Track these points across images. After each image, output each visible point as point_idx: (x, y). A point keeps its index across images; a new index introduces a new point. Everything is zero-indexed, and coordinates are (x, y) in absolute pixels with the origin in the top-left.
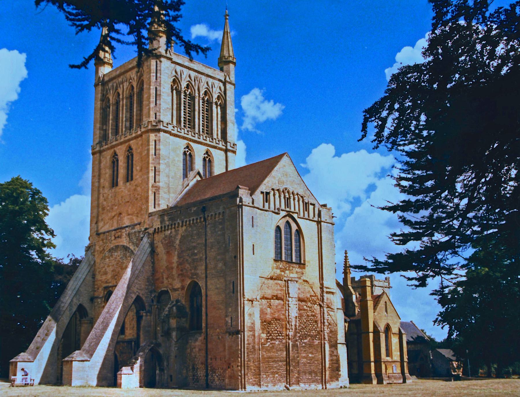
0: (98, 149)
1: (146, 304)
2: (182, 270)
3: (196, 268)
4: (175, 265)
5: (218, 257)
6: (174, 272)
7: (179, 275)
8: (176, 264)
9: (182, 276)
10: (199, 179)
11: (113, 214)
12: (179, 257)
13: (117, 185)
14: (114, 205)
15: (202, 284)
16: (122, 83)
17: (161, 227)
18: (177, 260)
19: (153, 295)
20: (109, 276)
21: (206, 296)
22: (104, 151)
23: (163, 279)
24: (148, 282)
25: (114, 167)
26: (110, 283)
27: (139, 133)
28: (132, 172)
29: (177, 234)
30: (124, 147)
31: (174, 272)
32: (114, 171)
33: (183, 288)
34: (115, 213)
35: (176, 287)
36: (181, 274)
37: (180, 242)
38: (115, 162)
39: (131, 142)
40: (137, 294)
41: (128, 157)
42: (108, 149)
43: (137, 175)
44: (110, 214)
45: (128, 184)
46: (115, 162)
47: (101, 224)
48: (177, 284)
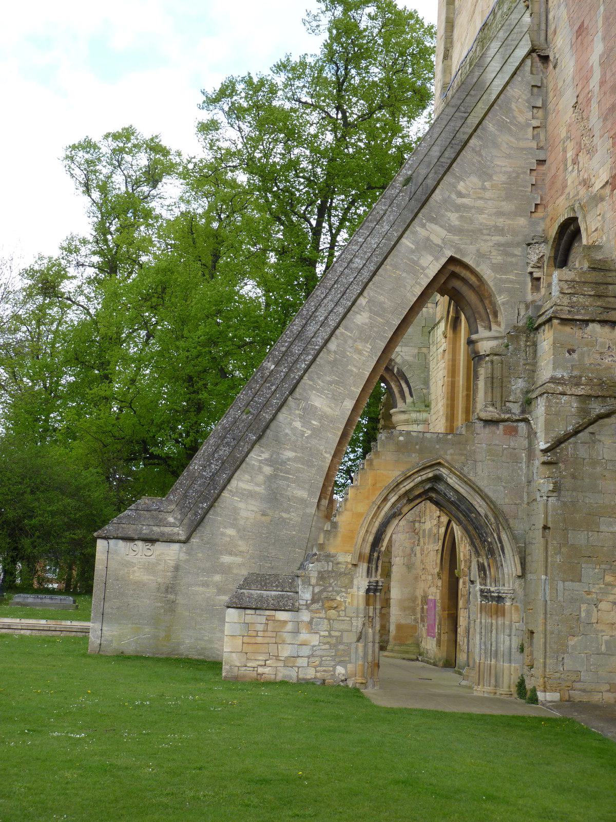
1: (500, 299)
19: (534, 258)
24: (508, 197)
40: (449, 253)
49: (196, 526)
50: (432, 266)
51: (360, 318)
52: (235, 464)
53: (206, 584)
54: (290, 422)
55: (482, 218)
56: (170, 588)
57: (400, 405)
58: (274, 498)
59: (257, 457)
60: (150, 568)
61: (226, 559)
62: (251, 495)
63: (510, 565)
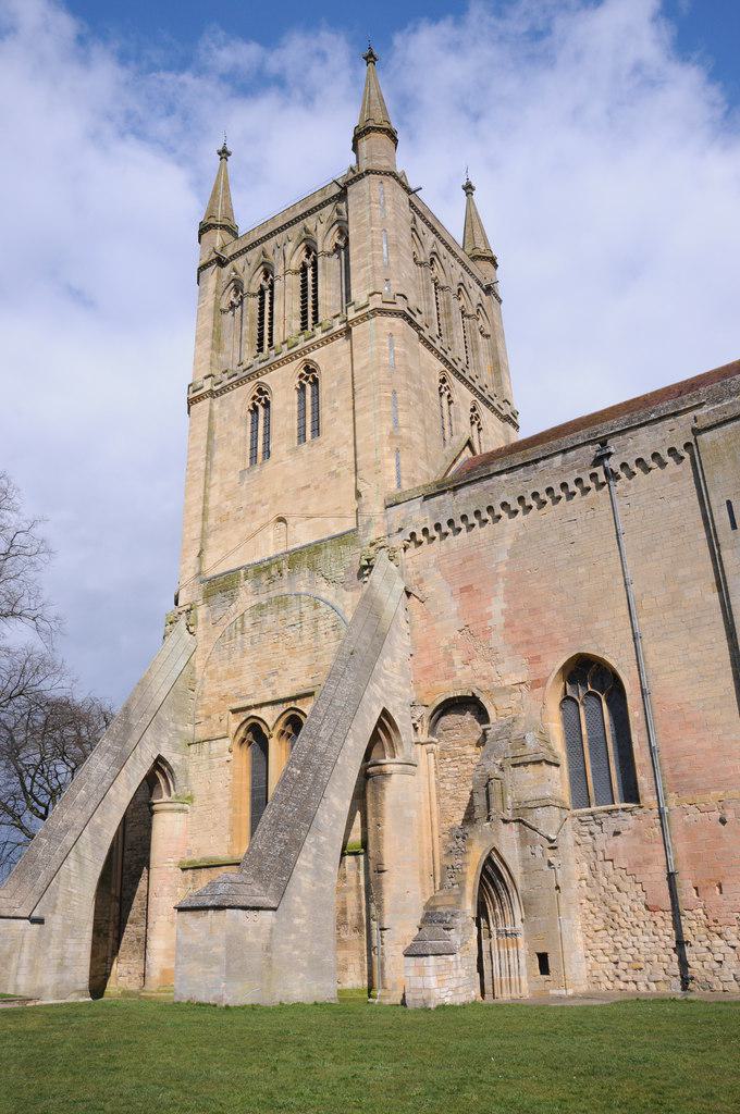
2: (528, 632)
4: (498, 620)
5: (681, 572)
6: (497, 640)
8: (502, 620)
9: (529, 647)
10: (471, 456)
11: (256, 525)
12: (510, 594)
13: (267, 453)
14: (260, 502)
15: (619, 659)
18: (504, 606)
20: (247, 680)
21: (643, 693)
22: (225, 390)
23: (451, 663)
25: (255, 422)
26: (248, 697)
27: (338, 327)
31: (497, 640)
32: (254, 431)
33: (537, 683)
34: (263, 521)
35: (507, 682)
36: (527, 642)
37: (513, 554)
40: (383, 705)
42: (239, 383)
43: (333, 421)
44: (243, 528)
47: (211, 558)
49: (281, 894)
50: (378, 713)
51: (350, 742)
52: (298, 845)
53: (287, 943)
54: (323, 817)
55: (395, 686)
56: (268, 949)
57: (165, 797)
58: (318, 873)
59: (310, 840)
60: (257, 931)
61: (297, 921)
62: (307, 869)
63: (518, 915)
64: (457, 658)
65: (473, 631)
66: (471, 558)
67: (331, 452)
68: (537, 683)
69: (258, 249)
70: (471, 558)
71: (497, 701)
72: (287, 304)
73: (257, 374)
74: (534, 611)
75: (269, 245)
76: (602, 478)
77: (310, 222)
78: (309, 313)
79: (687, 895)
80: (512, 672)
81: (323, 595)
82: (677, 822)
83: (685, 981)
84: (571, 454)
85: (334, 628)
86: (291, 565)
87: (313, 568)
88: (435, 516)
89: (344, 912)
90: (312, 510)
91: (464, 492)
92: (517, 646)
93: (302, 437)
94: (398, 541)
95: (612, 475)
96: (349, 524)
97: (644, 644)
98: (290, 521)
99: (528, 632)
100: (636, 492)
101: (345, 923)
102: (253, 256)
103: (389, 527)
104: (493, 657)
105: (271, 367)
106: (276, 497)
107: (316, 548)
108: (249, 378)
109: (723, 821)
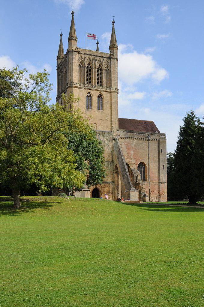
0: (78, 85)
3: (143, 158)
4: (132, 154)
5: (155, 155)
6: (132, 157)
7: (134, 158)
9: (136, 159)
12: (134, 151)
13: (91, 108)
15: (146, 164)
16: (95, 60)
17: (125, 137)
21: (149, 169)
27: (108, 90)
28: (102, 106)
29: (134, 142)
30: (98, 93)
33: (136, 164)
36: (136, 158)
38: (89, 96)
39: (102, 92)
41: (99, 98)
42: (85, 89)
43: (107, 109)
45: (100, 111)
46: (89, 96)
48: (133, 162)
64: (126, 158)
65: (129, 155)
66: (129, 144)
67: (106, 115)
68: (136, 164)
69: (88, 56)
70: (129, 144)
71: (131, 165)
72: (95, 76)
73: (89, 89)
74: (137, 154)
75: (91, 57)
76: (148, 140)
77: (102, 59)
78: (100, 82)
79: (151, 192)
80: (133, 162)
81: (105, 141)
82: (150, 184)
83: (149, 201)
84: (145, 134)
85: (108, 148)
86: (99, 134)
87: (104, 136)
88: (125, 135)
89: (110, 191)
90: (102, 125)
91: (130, 134)
92: (134, 158)
93: (99, 109)
94: (119, 137)
95: (149, 139)
96: (109, 130)
97: (150, 163)
98: (98, 125)
99: (136, 157)
100: (151, 142)
101: (110, 193)
102: (87, 57)
103: (117, 134)
104: (131, 159)
105: (93, 90)
106: (94, 119)
107: (104, 133)
108: (87, 89)
109: (155, 184)
